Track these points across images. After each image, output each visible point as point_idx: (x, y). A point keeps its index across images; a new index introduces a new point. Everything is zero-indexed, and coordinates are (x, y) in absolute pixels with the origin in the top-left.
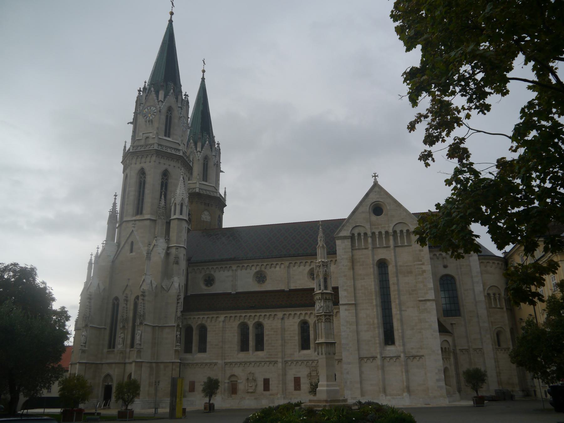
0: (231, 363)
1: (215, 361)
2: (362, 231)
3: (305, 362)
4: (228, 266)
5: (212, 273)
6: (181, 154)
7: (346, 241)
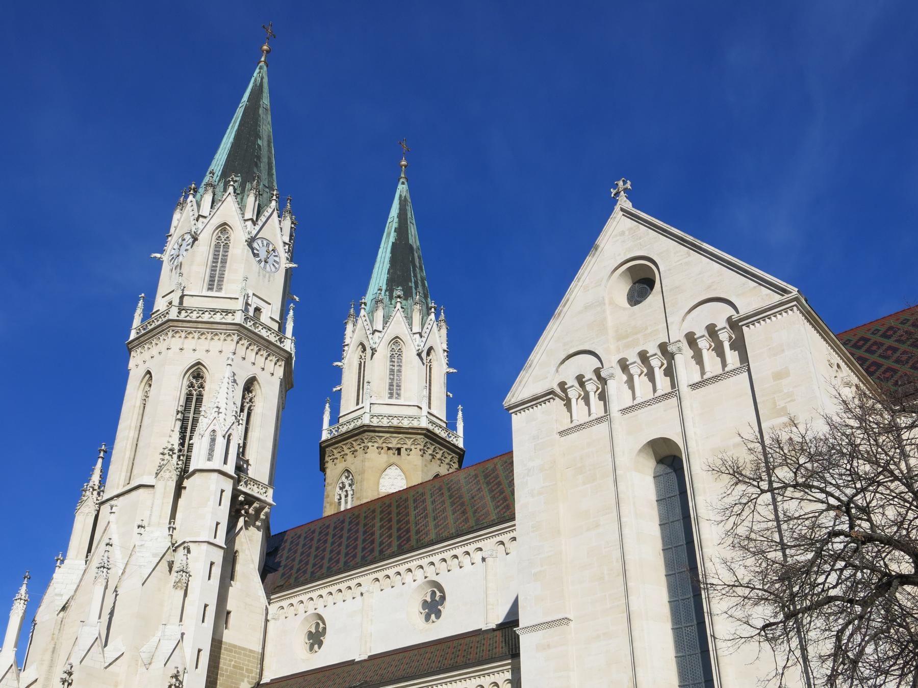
4: (352, 583)
6: (239, 318)
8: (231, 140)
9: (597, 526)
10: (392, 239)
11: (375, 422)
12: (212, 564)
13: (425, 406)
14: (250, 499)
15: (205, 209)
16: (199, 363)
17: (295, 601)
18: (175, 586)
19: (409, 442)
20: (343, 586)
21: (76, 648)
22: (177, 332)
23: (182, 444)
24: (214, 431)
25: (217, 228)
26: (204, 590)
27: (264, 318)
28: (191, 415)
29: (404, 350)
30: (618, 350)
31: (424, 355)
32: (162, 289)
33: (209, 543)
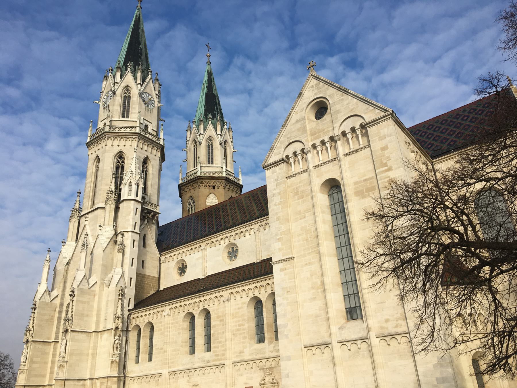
0: (175, 372)
1: (159, 371)
2: (297, 147)
3: (258, 362)
4: (197, 246)
5: (184, 258)
7: (277, 169)
8: (127, 45)
9: (305, 217)
10: (205, 91)
11: (203, 175)
12: (134, 241)
13: (224, 167)
14: (149, 212)
15: (118, 79)
16: (121, 152)
17: (172, 254)
18: (118, 252)
19: (218, 183)
20: (193, 247)
21: (75, 281)
22: (110, 138)
23: (116, 189)
24: (131, 182)
25: (124, 88)
26: (131, 252)
27: (150, 130)
28: (119, 175)
29: (214, 142)
30: (312, 140)
31: (223, 144)
32: (101, 118)
33: (132, 232)
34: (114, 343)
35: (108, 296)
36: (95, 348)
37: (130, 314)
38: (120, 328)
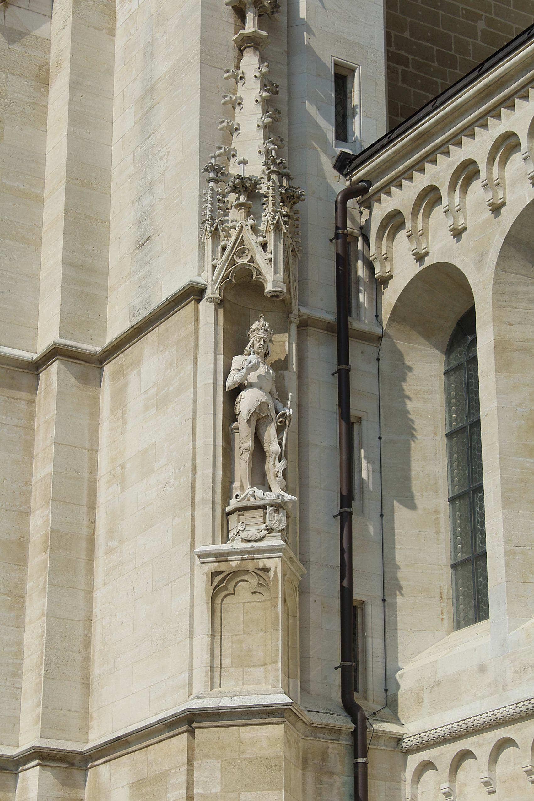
34: (231, 416)
35: (149, 54)
36: (78, 491)
37: (361, 192)
38: (272, 280)
